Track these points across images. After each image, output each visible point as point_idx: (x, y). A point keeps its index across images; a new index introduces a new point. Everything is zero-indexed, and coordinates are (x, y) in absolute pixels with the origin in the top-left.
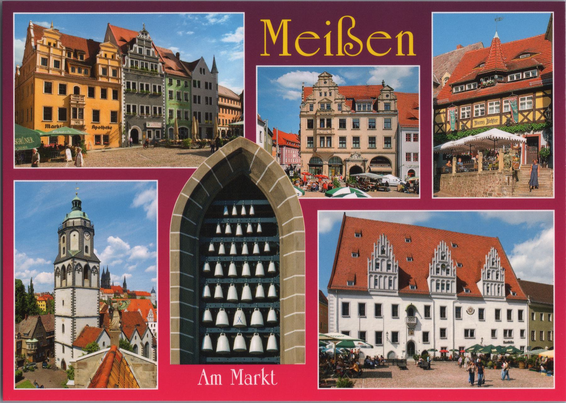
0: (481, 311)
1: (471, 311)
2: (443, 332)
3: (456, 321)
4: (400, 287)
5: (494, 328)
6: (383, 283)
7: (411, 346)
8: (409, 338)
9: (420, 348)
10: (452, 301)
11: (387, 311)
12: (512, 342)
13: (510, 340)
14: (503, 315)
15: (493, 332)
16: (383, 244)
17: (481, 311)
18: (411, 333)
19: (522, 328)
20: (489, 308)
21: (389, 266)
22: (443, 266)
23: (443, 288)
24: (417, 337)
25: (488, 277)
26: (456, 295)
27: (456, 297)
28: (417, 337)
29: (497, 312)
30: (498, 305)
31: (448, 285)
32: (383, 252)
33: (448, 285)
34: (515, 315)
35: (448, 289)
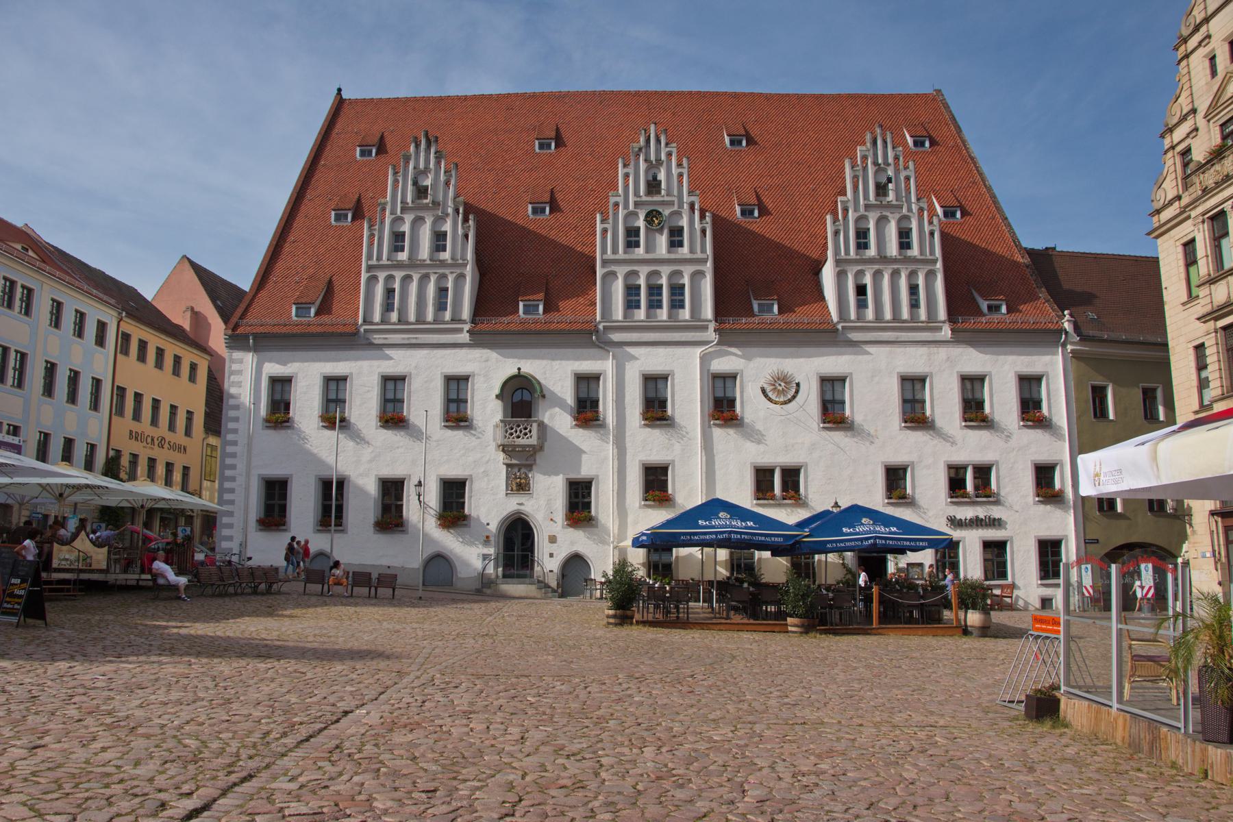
0: (832, 386)
1: (783, 390)
2: (656, 481)
3: (718, 433)
4: (481, 308)
5: (897, 459)
6: (417, 296)
7: (517, 539)
8: (512, 505)
9: (555, 544)
10: (698, 351)
11: (425, 404)
12: (995, 523)
13: (981, 512)
14: (944, 402)
15: (895, 477)
16: (422, 166)
17: (832, 386)
18: (519, 485)
19: (1044, 457)
20: (873, 376)
21: (439, 239)
22: (652, 216)
23: (654, 304)
24: (545, 503)
25: (862, 245)
26: (712, 326)
27: (711, 335)
28: (545, 503)
29: (913, 385)
30: (913, 360)
31: (677, 290)
32: (421, 192)
33: (677, 290)
34: (1002, 400)
35: (677, 304)
